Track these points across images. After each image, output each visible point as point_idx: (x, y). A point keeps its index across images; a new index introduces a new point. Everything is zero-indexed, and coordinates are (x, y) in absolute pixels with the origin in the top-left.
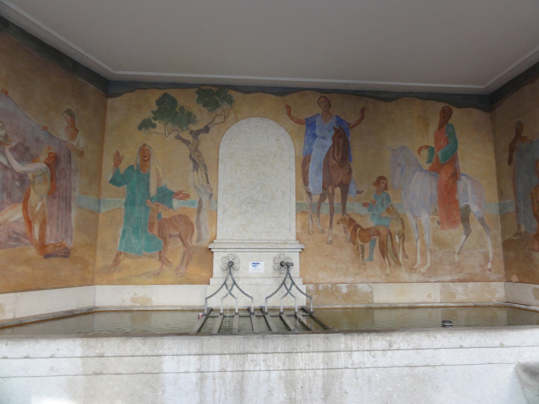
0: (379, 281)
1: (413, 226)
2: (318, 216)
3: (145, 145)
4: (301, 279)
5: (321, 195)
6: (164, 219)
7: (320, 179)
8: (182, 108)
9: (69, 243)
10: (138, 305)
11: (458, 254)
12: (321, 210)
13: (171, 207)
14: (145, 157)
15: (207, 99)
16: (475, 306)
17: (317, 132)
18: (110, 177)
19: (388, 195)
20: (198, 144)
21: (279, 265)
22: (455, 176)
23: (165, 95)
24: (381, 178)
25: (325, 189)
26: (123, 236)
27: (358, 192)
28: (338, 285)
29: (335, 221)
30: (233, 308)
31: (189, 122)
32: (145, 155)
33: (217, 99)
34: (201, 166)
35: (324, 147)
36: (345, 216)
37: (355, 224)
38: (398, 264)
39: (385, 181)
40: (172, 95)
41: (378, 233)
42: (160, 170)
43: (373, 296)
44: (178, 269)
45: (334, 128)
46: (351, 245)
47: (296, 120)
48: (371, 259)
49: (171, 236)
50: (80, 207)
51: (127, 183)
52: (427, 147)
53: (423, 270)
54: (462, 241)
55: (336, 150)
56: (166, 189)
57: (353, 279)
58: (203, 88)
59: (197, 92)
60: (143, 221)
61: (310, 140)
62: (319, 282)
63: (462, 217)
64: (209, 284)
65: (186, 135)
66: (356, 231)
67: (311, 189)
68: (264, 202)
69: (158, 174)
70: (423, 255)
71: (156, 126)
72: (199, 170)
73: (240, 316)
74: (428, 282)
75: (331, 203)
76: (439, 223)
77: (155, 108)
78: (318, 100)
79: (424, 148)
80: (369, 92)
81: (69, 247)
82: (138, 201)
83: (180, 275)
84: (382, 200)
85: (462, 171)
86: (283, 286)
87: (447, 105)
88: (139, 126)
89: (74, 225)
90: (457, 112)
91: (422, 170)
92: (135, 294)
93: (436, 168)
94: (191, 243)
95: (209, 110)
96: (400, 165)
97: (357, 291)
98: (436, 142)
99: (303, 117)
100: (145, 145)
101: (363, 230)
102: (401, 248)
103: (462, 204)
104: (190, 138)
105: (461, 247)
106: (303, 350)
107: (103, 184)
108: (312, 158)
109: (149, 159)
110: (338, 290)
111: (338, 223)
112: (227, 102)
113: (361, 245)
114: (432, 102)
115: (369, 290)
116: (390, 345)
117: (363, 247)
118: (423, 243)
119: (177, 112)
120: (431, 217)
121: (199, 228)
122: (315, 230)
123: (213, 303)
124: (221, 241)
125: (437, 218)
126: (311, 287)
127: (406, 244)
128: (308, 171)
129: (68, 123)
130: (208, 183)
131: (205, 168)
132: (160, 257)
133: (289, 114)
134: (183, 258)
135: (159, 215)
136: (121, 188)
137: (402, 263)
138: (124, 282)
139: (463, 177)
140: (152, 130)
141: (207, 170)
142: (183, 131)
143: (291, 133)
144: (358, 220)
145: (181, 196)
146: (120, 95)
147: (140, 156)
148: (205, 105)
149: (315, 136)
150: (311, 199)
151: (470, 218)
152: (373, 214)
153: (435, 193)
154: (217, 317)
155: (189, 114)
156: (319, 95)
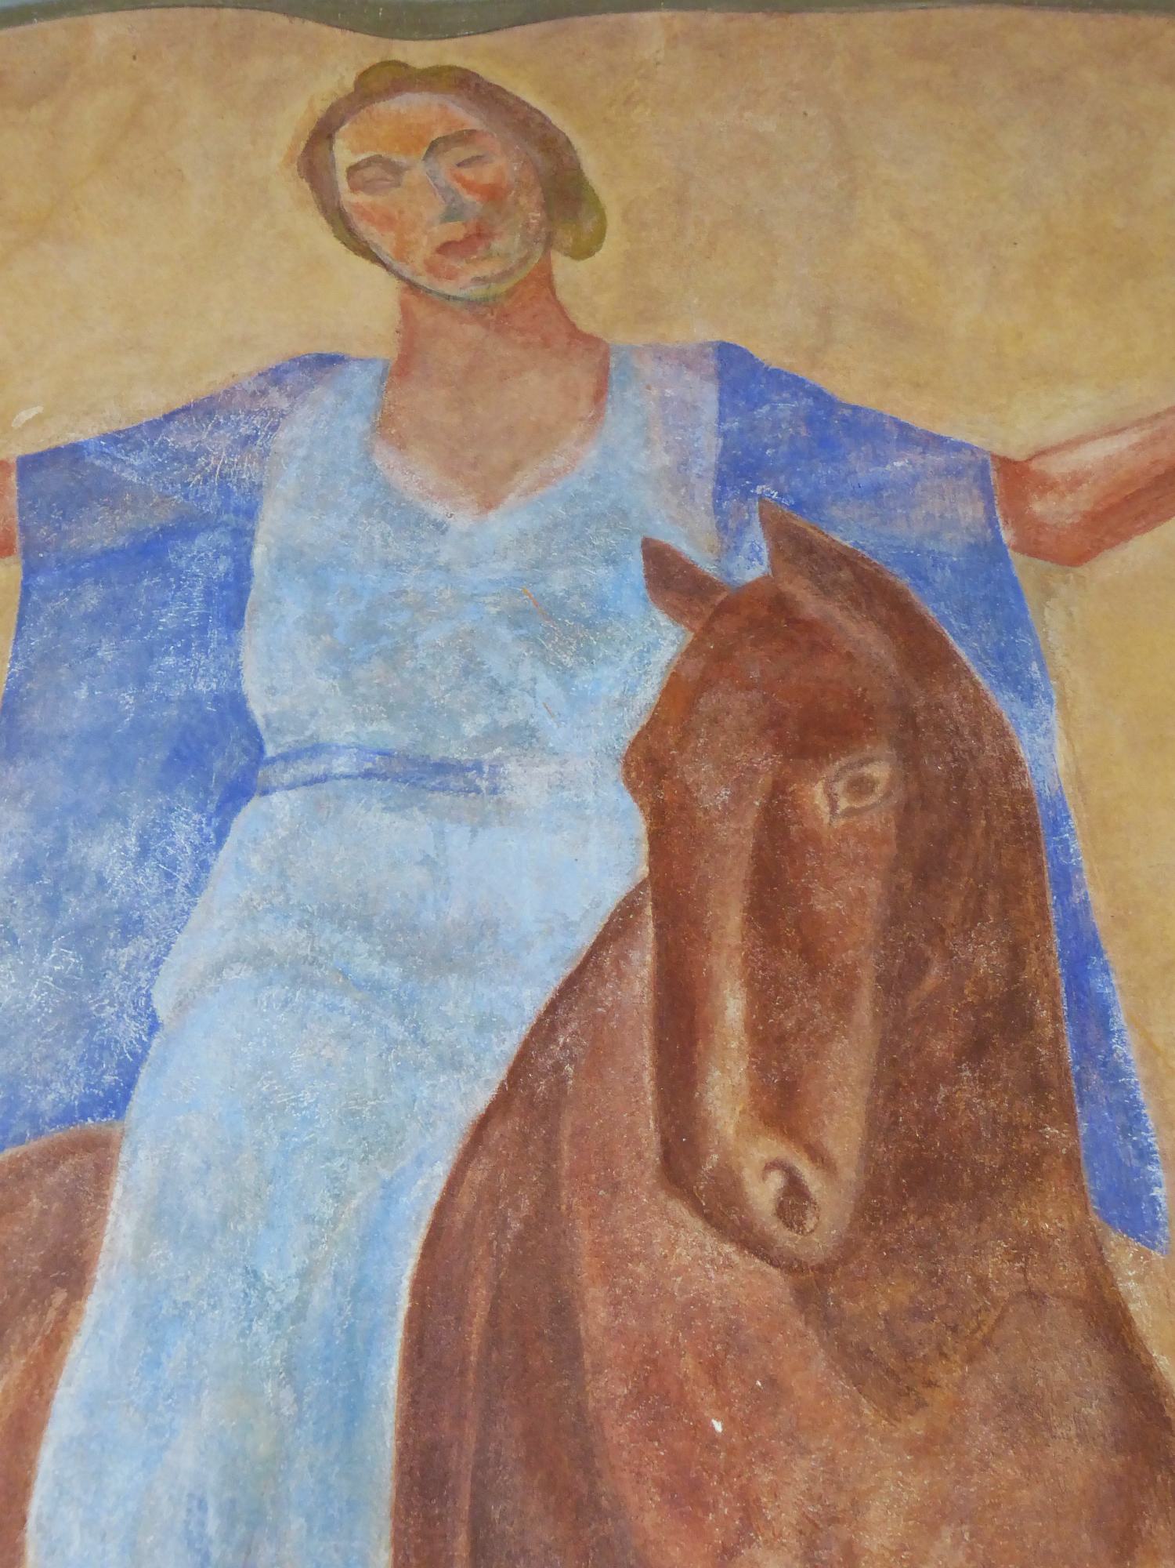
17: (279, 671)
35: (439, 953)
45: (667, 575)
55: (732, 1006)
61: (106, 853)
78: (323, 132)
108: (121, 1228)
149: (220, 760)
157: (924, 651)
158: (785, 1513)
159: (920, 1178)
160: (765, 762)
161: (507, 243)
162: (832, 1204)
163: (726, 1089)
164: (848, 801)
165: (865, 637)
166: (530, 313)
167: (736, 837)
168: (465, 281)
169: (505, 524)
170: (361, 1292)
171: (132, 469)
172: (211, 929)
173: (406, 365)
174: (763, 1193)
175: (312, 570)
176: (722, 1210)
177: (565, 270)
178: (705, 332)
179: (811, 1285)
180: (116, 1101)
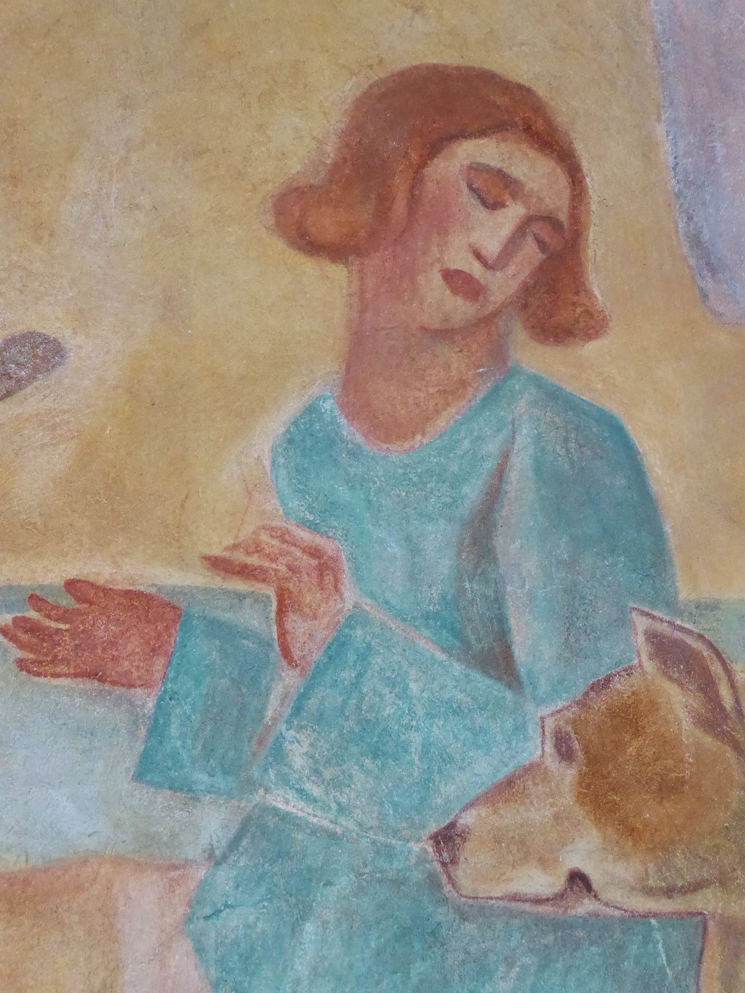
24: (434, 109)
39: (533, 170)
84: (480, 537)
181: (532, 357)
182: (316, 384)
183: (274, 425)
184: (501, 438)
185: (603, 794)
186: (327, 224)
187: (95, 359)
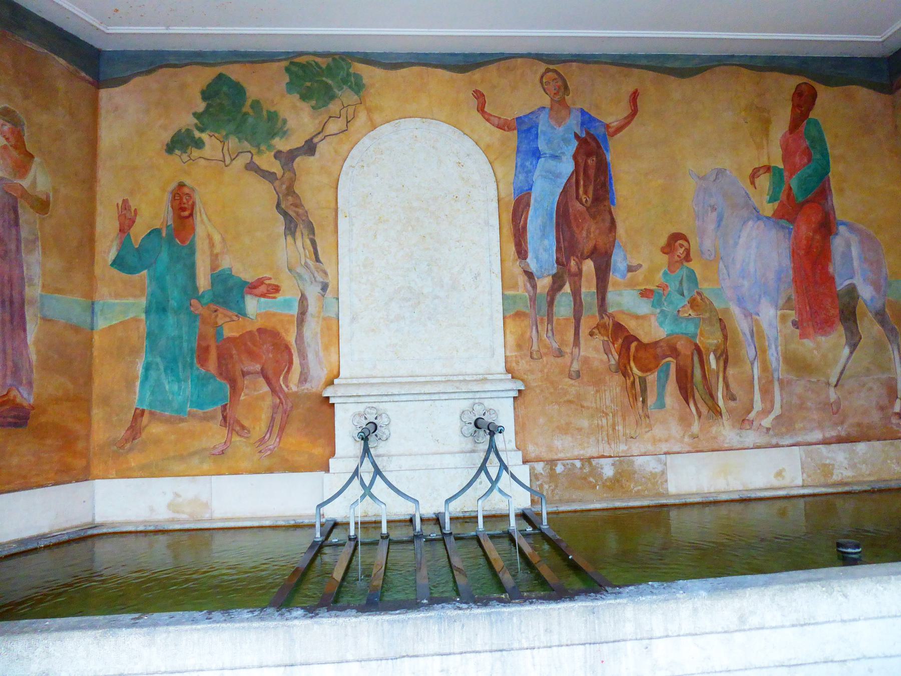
0: (679, 450)
1: (744, 334)
2: (550, 321)
3: (181, 185)
4: (520, 453)
5: (554, 276)
6: (230, 340)
7: (551, 242)
8: (256, 105)
9: (25, 395)
10: (184, 516)
11: (836, 386)
12: (555, 309)
13: (242, 313)
14: (184, 209)
15: (308, 84)
16: (872, 492)
17: (542, 145)
18: (112, 255)
19: (692, 272)
20: (292, 181)
21: (472, 428)
22: (827, 226)
23: (220, 78)
24: (676, 237)
25: (563, 265)
26: (146, 377)
27: (630, 269)
28: (594, 462)
29: (584, 331)
30: (378, 519)
31: (273, 135)
32: (183, 207)
33: (330, 82)
34: (301, 226)
35: (558, 176)
36: (606, 318)
37: (626, 334)
38: (716, 411)
39: (685, 244)
40: (233, 77)
41: (674, 351)
42: (217, 238)
43: (666, 481)
44: (262, 440)
45: (577, 136)
46: (618, 378)
47: (496, 121)
48: (662, 406)
49: (244, 374)
50: (45, 319)
51: (147, 267)
52: (768, 169)
53: (767, 422)
54: (843, 361)
55: (582, 183)
56: (231, 276)
57: (625, 448)
58: (297, 60)
59: (287, 70)
60: (185, 345)
61: (528, 164)
62: (555, 457)
63: (842, 312)
64: (327, 470)
65: (267, 162)
66: (628, 349)
67: (532, 264)
68: (437, 297)
69: (212, 245)
70: (766, 392)
71: (203, 143)
72: (298, 234)
73: (391, 542)
74: (777, 446)
75: (576, 293)
76: (794, 324)
77: (201, 106)
78: (542, 77)
79: (761, 172)
80: (647, 57)
81: (25, 404)
82: (173, 303)
83: (269, 452)
84: (681, 283)
85: (839, 216)
86: (483, 474)
87: (805, 80)
88: (167, 145)
89: (34, 357)
90: (825, 95)
91: (759, 217)
92: (177, 495)
93: (788, 211)
94: (287, 387)
95: (313, 107)
96: (714, 209)
97: (635, 472)
98: (784, 159)
99: (511, 114)
100: (181, 185)
101: (642, 346)
102: (721, 379)
103: (841, 284)
104: (276, 168)
105: (842, 373)
106: (537, 644)
107: (98, 270)
108: (532, 201)
109: (191, 215)
110: (595, 472)
111: (591, 334)
112: (350, 87)
113: (640, 377)
114: (776, 74)
115: (659, 468)
116: (742, 619)
117: (643, 381)
118: (765, 368)
119: (246, 114)
120: (779, 313)
121: (303, 356)
122: (543, 350)
123: (335, 511)
124: (349, 381)
125: (793, 315)
126: (539, 467)
127: (731, 371)
128: (525, 227)
129: (7, 139)
130: (317, 260)
131: (312, 231)
132: (225, 418)
133: (481, 109)
134: (273, 419)
135: (218, 328)
136: (136, 277)
137: (724, 411)
138: (151, 471)
139: (842, 229)
140: (196, 153)
141: (314, 234)
142: (260, 152)
143: (486, 150)
144: (632, 326)
145: (262, 289)
146: (124, 81)
147: (172, 207)
148: (304, 97)
149: (536, 154)
150: (534, 287)
151: (858, 311)
152: (662, 311)
153: (787, 262)
154: (343, 545)
155: (273, 117)
156: (543, 67)
157: (599, 147)
158: (585, 228)
159: (597, 200)
160: (584, 157)
161: (561, 93)
162: (590, 201)
163: (581, 191)
164: (592, 161)
165: (593, 144)
166: (562, 103)
167: (582, 165)
168: (557, 98)
169: (561, 129)
170: (552, 208)
171: (526, 120)
172: (537, 173)
173: (551, 109)
174: (584, 200)
175: (544, 133)
176: (581, 203)
177: (566, 97)
178: (578, 106)
179: (588, 209)
180: (531, 189)
181: (686, 264)
182: (665, 268)
183: (662, 272)
184: (682, 272)
185: (692, 307)
186: (666, 251)
187: (645, 266)
